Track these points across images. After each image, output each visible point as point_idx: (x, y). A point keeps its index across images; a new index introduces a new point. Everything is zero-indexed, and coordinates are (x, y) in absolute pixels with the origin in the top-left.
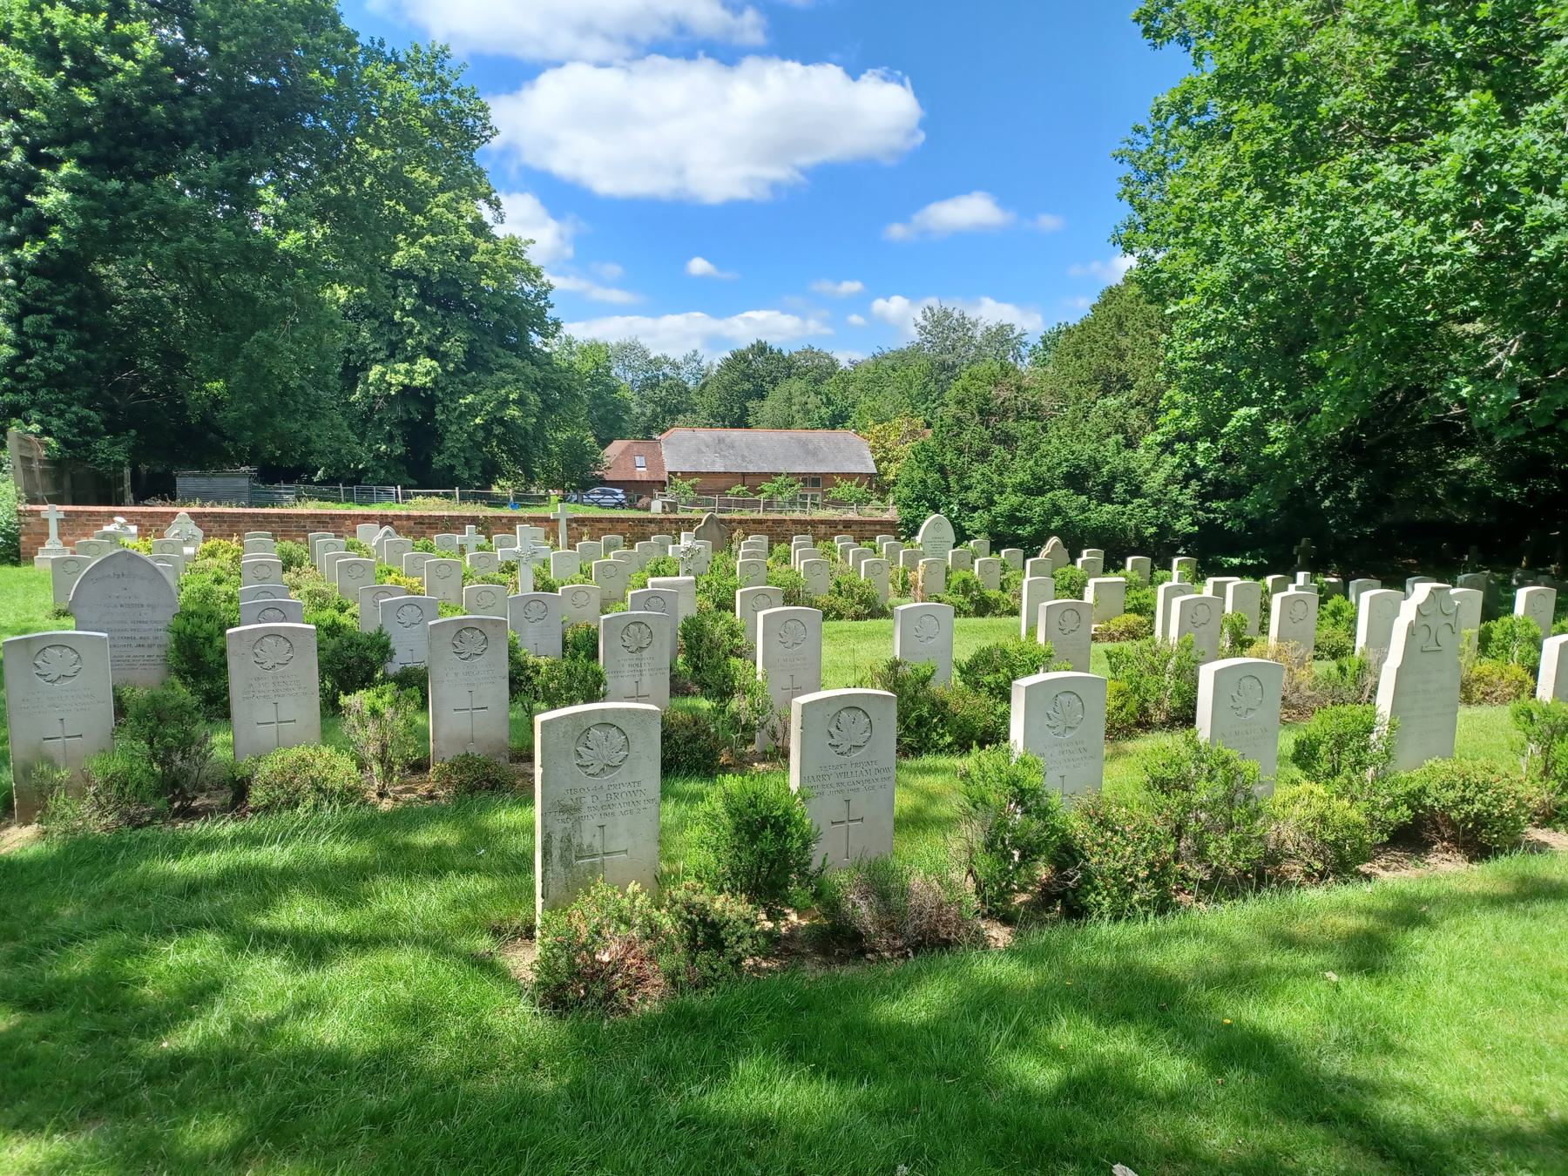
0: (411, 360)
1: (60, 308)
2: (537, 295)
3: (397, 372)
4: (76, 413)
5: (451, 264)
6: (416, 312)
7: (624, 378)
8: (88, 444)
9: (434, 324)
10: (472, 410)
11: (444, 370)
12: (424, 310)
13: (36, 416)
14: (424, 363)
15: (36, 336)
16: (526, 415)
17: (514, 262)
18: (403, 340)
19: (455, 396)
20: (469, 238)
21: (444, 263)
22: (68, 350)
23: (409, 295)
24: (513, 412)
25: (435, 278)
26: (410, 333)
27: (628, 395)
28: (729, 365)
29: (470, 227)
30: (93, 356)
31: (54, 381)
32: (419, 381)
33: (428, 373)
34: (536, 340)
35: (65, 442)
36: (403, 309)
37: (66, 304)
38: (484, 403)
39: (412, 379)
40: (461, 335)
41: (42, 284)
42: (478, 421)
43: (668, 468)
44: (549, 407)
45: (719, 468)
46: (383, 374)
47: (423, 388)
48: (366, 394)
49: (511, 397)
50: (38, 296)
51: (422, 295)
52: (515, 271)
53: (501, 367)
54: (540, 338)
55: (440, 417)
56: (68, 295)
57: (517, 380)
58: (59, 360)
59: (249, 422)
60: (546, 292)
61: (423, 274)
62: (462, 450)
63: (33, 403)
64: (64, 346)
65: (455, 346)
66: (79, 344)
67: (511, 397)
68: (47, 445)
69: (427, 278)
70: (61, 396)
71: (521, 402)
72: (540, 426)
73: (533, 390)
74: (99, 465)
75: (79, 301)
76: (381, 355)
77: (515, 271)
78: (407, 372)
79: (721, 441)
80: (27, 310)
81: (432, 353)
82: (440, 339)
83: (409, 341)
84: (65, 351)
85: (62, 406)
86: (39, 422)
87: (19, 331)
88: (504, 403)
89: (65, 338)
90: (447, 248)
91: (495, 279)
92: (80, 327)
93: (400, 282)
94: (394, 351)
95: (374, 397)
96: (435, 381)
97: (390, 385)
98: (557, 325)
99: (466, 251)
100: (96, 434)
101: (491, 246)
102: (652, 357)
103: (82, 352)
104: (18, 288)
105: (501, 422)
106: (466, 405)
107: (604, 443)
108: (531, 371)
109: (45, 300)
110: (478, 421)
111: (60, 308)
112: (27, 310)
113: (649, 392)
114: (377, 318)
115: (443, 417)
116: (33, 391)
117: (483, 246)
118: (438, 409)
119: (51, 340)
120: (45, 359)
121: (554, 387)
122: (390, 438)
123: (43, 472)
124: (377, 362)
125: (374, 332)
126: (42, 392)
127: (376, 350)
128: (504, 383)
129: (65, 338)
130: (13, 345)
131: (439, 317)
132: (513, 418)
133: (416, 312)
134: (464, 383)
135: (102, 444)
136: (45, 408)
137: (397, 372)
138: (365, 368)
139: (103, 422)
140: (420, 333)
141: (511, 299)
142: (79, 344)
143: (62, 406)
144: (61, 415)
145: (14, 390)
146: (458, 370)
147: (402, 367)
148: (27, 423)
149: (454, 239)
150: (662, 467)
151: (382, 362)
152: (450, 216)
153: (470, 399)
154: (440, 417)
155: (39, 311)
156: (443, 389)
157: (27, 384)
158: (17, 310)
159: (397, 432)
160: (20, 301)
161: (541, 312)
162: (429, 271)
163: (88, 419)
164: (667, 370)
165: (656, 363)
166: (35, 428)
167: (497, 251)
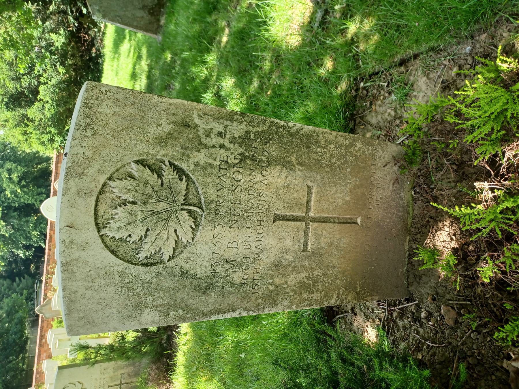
10: (14, 192)
24: (15, 176)
42: (19, 191)
48: (6, 231)
49: (7, 176)
55: (17, 205)
62: (33, 198)
67: (7, 176)
71: (10, 171)
88: (10, 179)
105: (19, 182)
106: (11, 194)
115: (17, 203)
122: (27, 222)
132: (18, 177)
153: (8, 193)
159: (24, 219)
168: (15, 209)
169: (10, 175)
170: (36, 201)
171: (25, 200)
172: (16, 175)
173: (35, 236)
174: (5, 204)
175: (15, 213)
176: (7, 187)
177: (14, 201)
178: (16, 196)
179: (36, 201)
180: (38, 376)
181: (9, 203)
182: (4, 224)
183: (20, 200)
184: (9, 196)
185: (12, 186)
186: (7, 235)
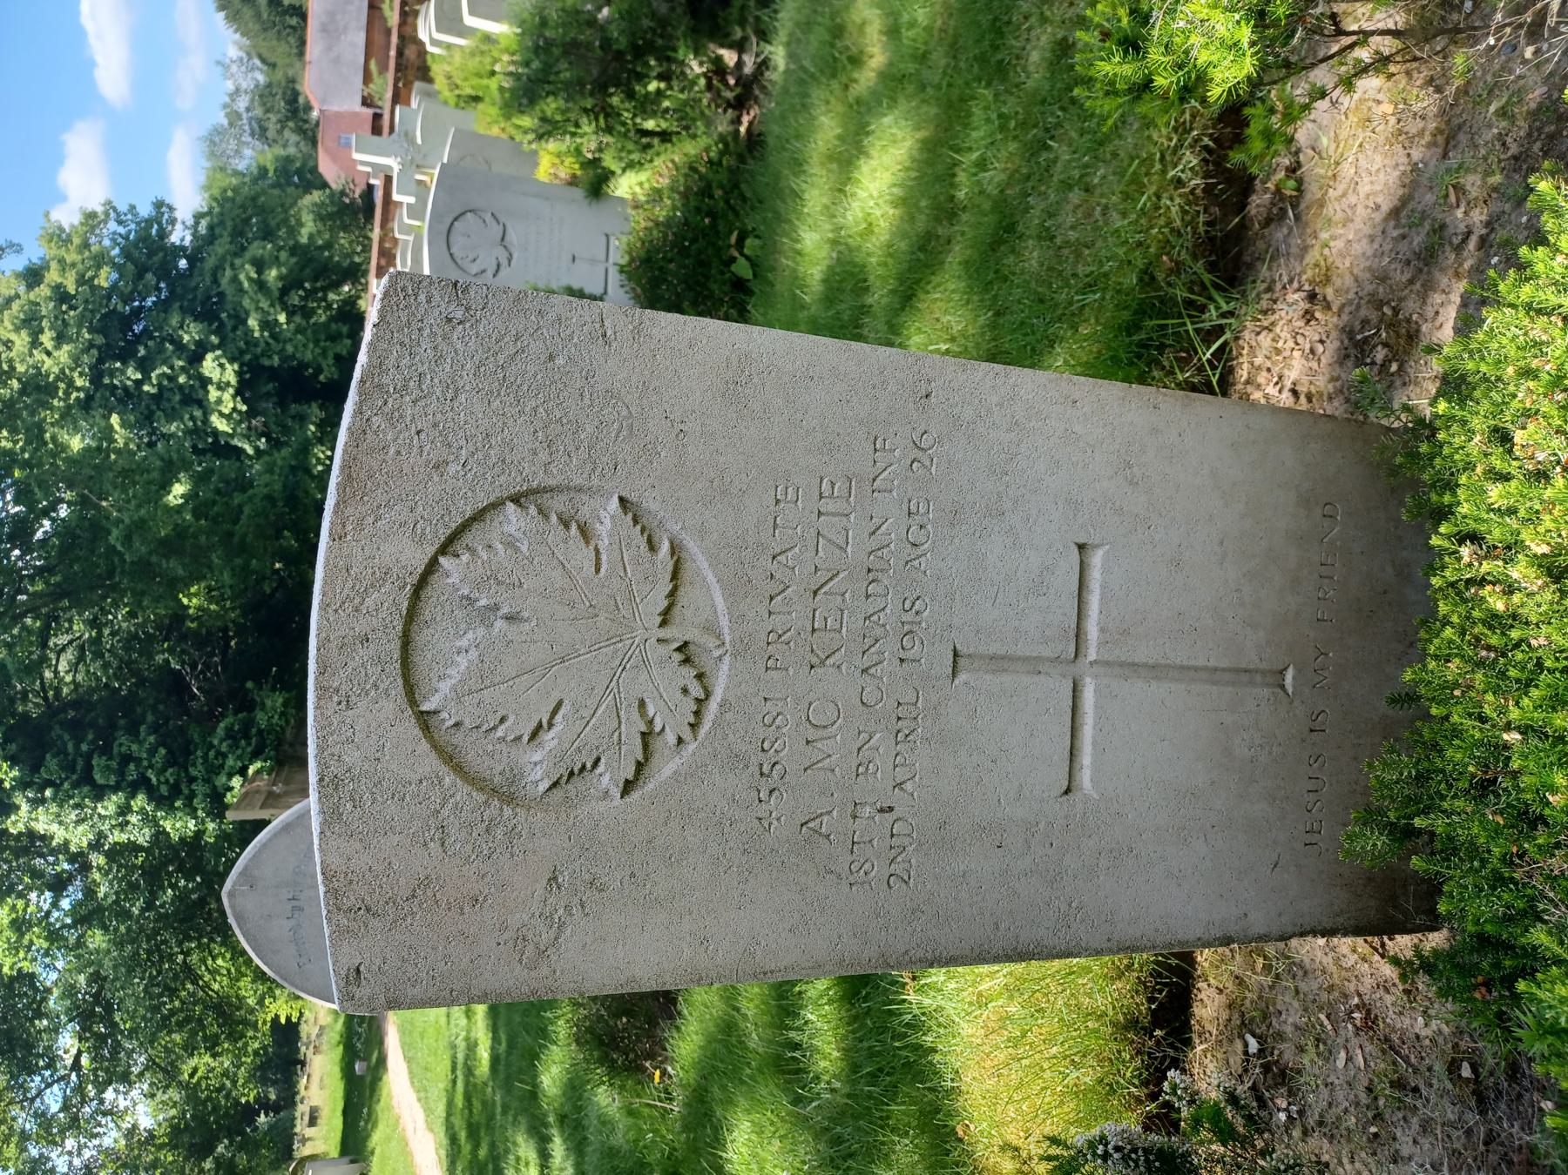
0: (208, 381)
1: (84, 747)
2: (120, 223)
3: (219, 401)
4: (221, 742)
5: (82, 317)
6: (145, 366)
7: (250, 156)
8: (260, 732)
9: (161, 350)
10: (266, 324)
11: (218, 347)
12: (144, 359)
13: (221, 780)
14: (209, 366)
15: (121, 773)
16: (276, 261)
17: (76, 241)
18: (181, 387)
19: (250, 342)
20: (43, 291)
21: (80, 326)
22: (140, 743)
23: (123, 372)
24: (272, 274)
25: (100, 340)
26: (172, 379)
27: (269, 156)
28: (234, 18)
29: (30, 287)
30: (150, 718)
31: (179, 756)
32: (230, 375)
33: (221, 366)
34: (180, 236)
35: (255, 755)
36: (139, 383)
37: (78, 741)
38: (258, 308)
39: (228, 384)
40: (174, 321)
41: (52, 763)
42: (282, 318)
43: (357, 107)
44: (267, 234)
45: (360, 38)
46: (221, 415)
47: (239, 374)
48: (248, 437)
50: (70, 767)
51: (125, 356)
52: (86, 245)
53: (216, 281)
54: (179, 226)
55: (276, 361)
56: (66, 737)
57: (232, 265)
58: (152, 752)
59: (239, 561)
60: (115, 209)
61: (95, 352)
63: (207, 781)
64: (134, 747)
65: (190, 334)
66: (133, 731)
67: (255, 276)
68: (258, 772)
69: (99, 348)
70: (199, 753)
71: (260, 265)
72: (295, 249)
73: (243, 249)
74: (287, 722)
75: (77, 728)
76: (198, 413)
77: (86, 245)
78: (219, 388)
79: (324, 29)
80: (87, 779)
81: (196, 358)
82: (180, 346)
83: (182, 380)
84: (142, 746)
85: (212, 754)
86: (230, 776)
87: (116, 789)
88: (261, 285)
89: (123, 744)
90: (58, 316)
91: (99, 267)
92: (113, 726)
93: (106, 381)
94: (195, 396)
95: (249, 428)
96: (232, 360)
97: (234, 409)
98: (159, 205)
99: (61, 296)
100: (247, 725)
101: (54, 265)
102: (225, 122)
103: (143, 728)
104: (56, 786)
105: (284, 292)
106: (262, 330)
107: (324, 185)
108: (222, 247)
109: (74, 761)
110: (282, 318)
111: (84, 747)
112: (87, 779)
113: (271, 134)
114: (152, 413)
115: (276, 358)
116: (192, 780)
117: (53, 276)
118: (266, 362)
119: (126, 759)
120: (151, 766)
121: (244, 215)
122: (302, 419)
123: (286, 783)
124: (206, 421)
125: (172, 416)
126: (193, 772)
127: (192, 418)
128: (235, 279)
129: (123, 744)
130: (133, 796)
131: (150, 343)
132: (280, 277)
133: (145, 366)
134: (235, 329)
135: (261, 719)
136: (213, 770)
137: (219, 401)
138: (215, 433)
139: (236, 713)
140: (172, 368)
141: (126, 253)
142: (133, 731)
143: (212, 754)
144: (224, 756)
145: (192, 795)
146: (219, 332)
147: (213, 394)
148: (231, 789)
149: (47, 309)
150: (356, 114)
151: (206, 415)
152: (15, 306)
153: (253, 323)
154: (276, 361)
155: (89, 768)
156: (242, 352)
157: (183, 787)
158: (86, 789)
160: (75, 785)
161: (149, 222)
162: (91, 345)
163: (229, 730)
164: (242, 104)
165: (234, 117)
166: (236, 782)
167: (61, 261)
168: (272, 373)
169: (259, 272)
170: (324, 353)
171: (296, 347)
172: (274, 273)
173: (318, 459)
174: (248, 357)
175: (270, 386)
176: (253, 307)
177: (267, 353)
178: (274, 336)
179: (324, 353)
180: (383, 262)
181: (256, 357)
182: (244, 408)
183: (283, 350)
184: (257, 334)
185: (264, 304)
186: (250, 451)
